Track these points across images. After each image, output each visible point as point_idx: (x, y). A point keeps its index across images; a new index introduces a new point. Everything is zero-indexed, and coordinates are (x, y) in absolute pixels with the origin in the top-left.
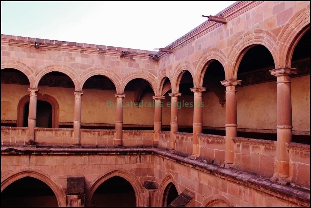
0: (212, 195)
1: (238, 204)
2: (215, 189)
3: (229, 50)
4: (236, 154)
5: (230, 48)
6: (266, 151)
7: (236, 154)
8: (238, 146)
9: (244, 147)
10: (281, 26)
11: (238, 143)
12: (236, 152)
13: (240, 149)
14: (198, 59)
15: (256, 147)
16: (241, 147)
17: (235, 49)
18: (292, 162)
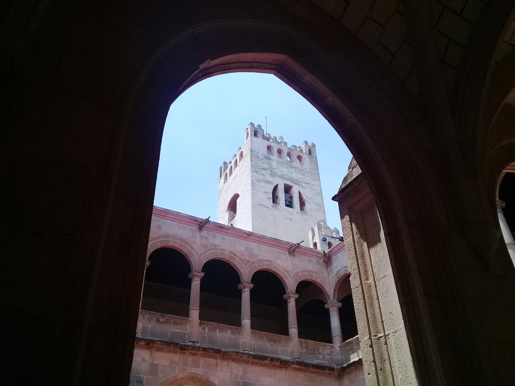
0: (176, 374)
1: (214, 376)
2: (181, 366)
3: (203, 251)
4: (200, 335)
5: (203, 250)
6: (232, 334)
7: (200, 335)
8: (204, 329)
9: (210, 330)
10: (250, 260)
11: (204, 326)
12: (200, 333)
13: (205, 331)
14: (155, 237)
15: (223, 331)
16: (206, 330)
17: (208, 253)
18: (253, 343)
